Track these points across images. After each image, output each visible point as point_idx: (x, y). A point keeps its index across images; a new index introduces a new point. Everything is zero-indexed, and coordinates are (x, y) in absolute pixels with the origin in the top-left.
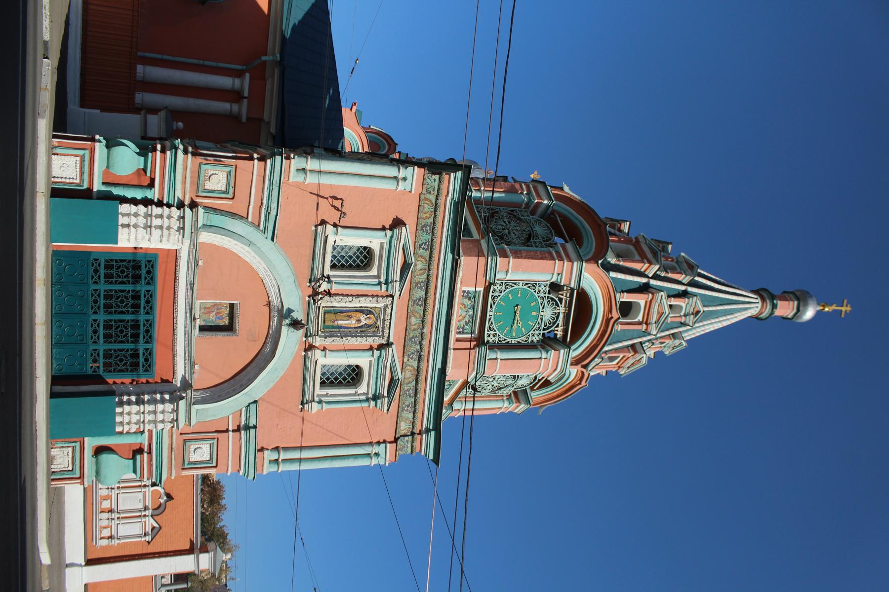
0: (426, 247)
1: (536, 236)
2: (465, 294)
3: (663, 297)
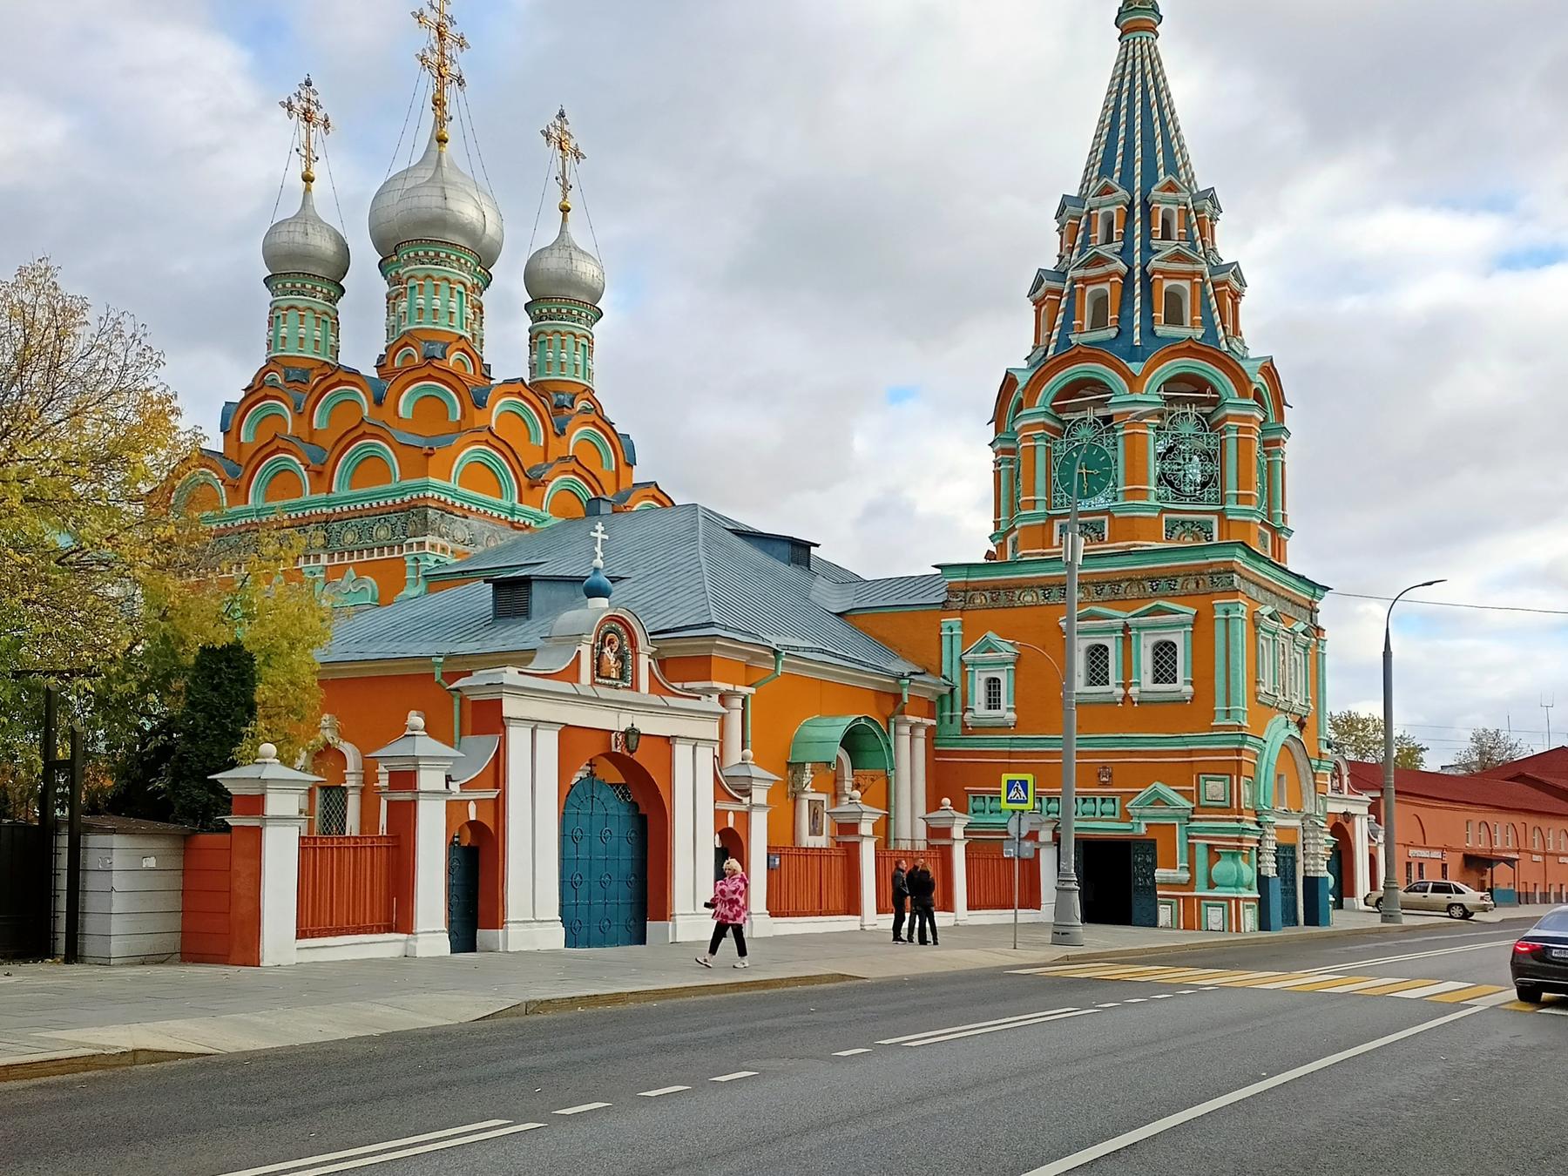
2: (1169, 534)
3: (1157, 258)
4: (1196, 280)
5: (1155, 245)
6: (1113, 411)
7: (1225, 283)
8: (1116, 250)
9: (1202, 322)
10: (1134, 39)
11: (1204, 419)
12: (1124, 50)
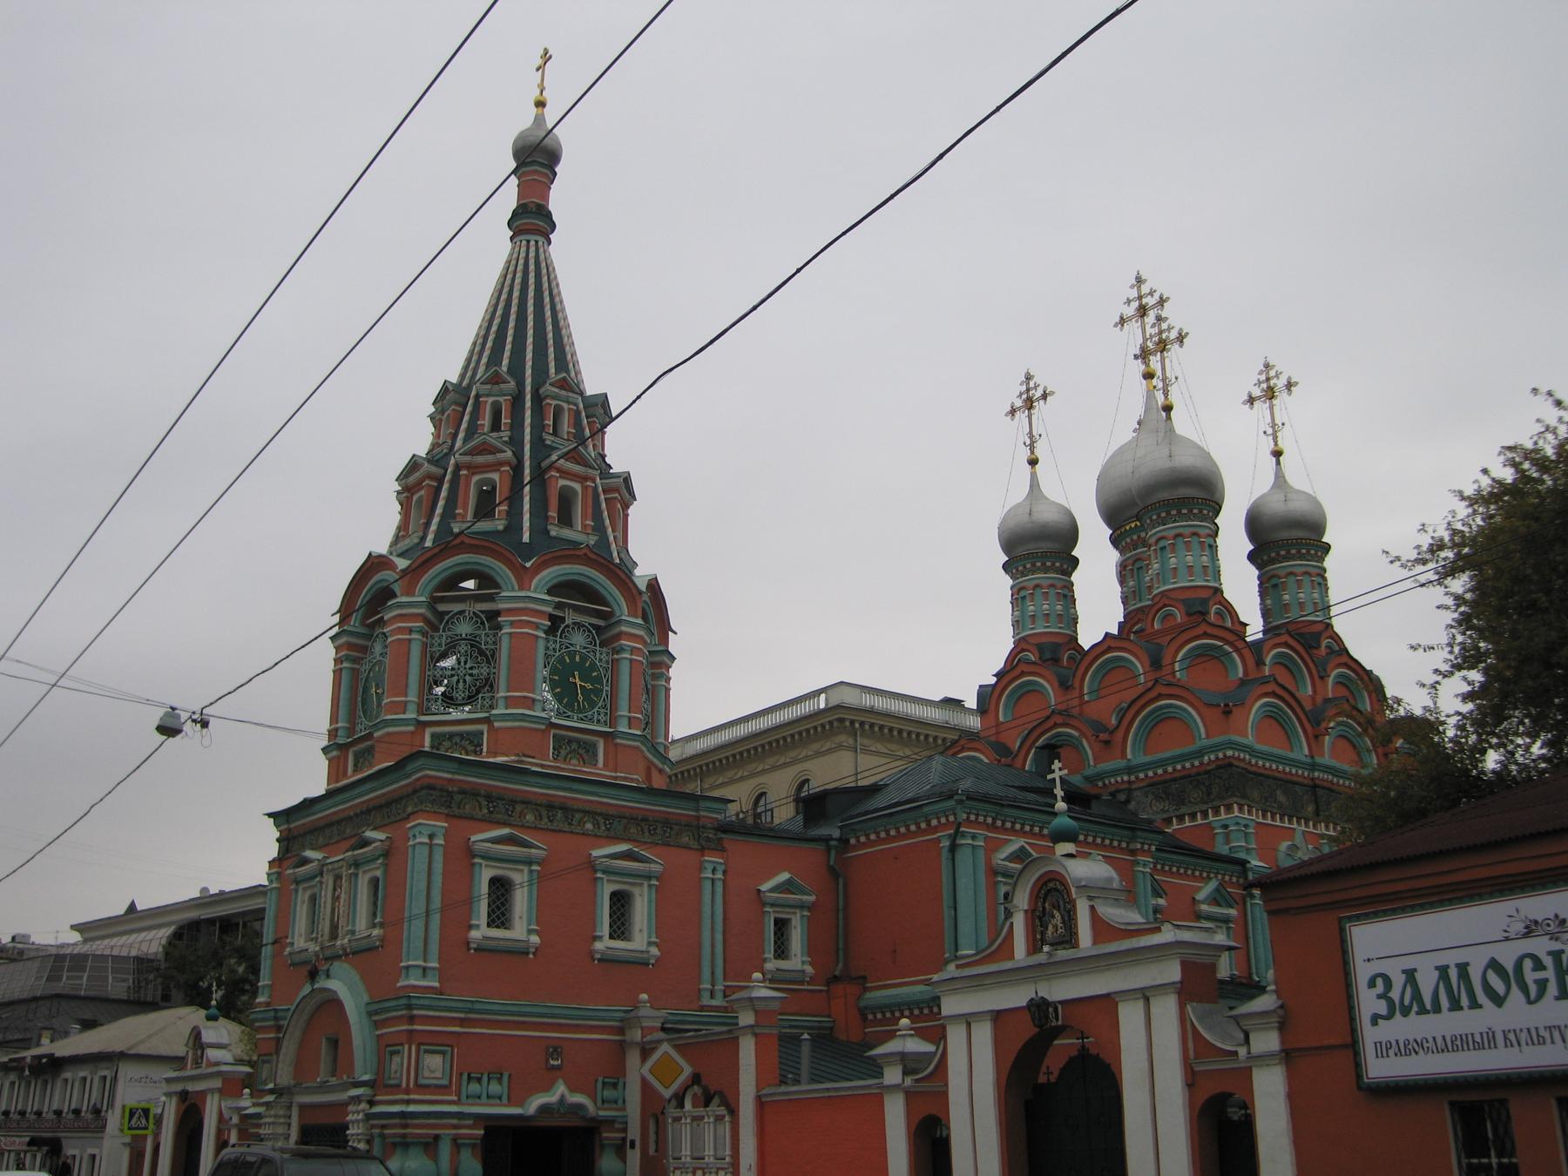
0: (511, 808)
1: (476, 637)
4: (588, 483)
5: (549, 440)
6: (502, 606)
7: (617, 490)
8: (504, 439)
9: (594, 529)
10: (528, 241)
11: (594, 632)
12: (517, 249)
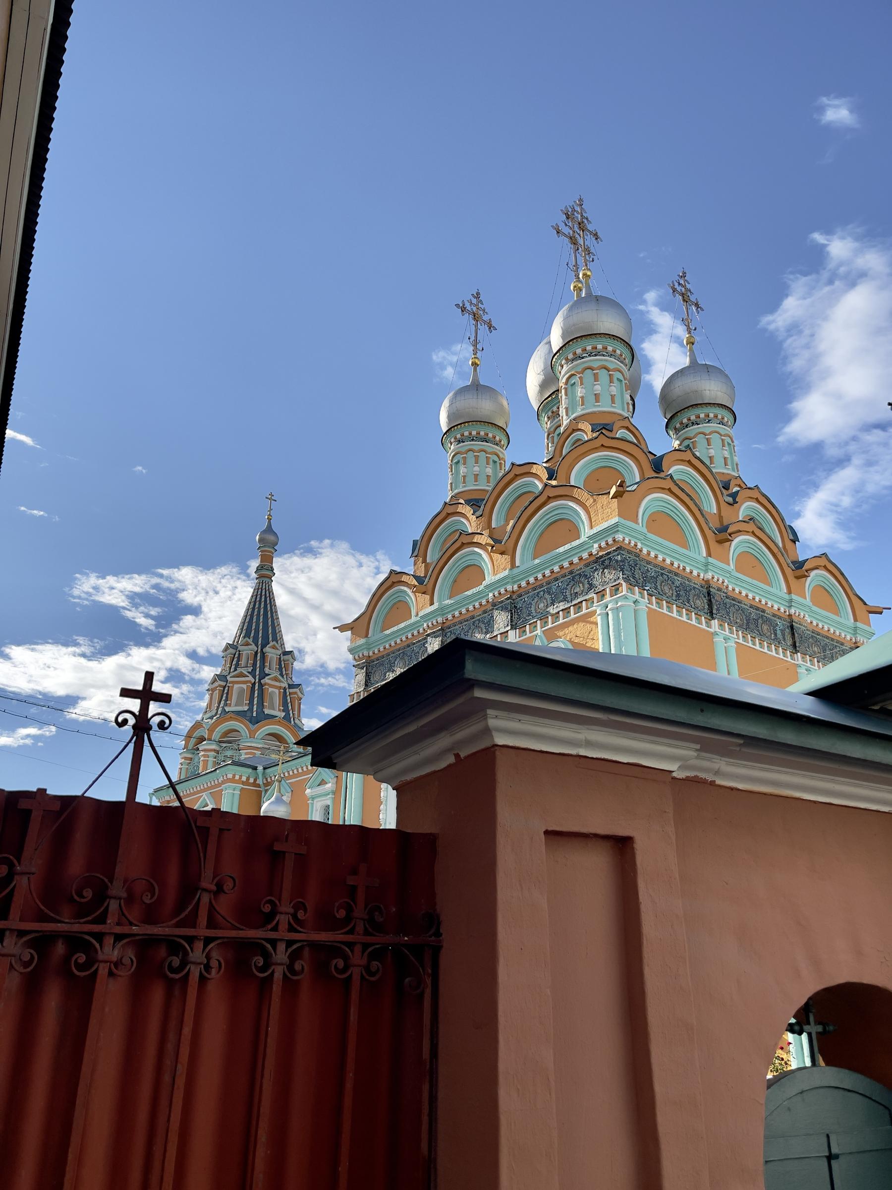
7: (295, 693)
